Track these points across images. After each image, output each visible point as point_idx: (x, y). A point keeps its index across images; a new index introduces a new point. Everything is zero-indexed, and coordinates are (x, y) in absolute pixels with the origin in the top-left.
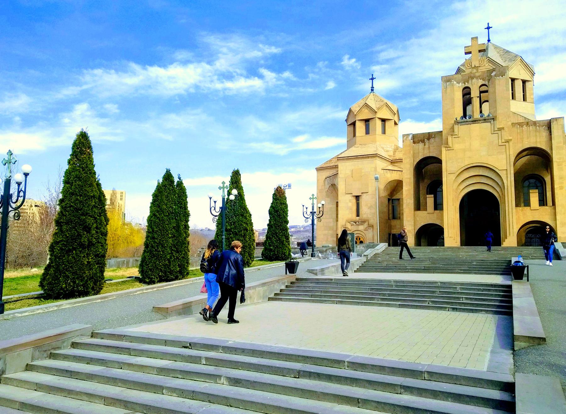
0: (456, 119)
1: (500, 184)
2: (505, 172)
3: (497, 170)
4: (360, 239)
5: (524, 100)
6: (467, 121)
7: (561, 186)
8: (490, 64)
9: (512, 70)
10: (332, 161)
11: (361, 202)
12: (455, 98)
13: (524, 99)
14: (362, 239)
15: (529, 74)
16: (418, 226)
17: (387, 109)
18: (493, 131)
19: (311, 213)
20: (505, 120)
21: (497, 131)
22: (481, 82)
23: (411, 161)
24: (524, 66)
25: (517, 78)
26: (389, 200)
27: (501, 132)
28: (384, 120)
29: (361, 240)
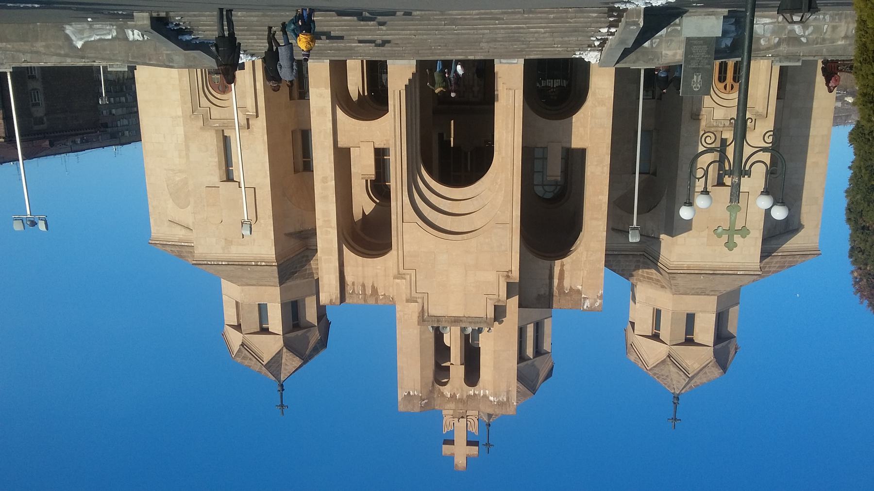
0: (490, 329)
1: (416, 196)
4: (725, 87)
6: (470, 323)
7: (324, 183)
10: (777, 265)
12: (492, 369)
14: (722, 85)
16: (582, 115)
17: (645, 357)
18: (426, 298)
19: (748, 173)
20: (406, 314)
21: (419, 298)
22: (447, 391)
23: (587, 254)
26: (654, 174)
28: (656, 337)
29: (724, 84)
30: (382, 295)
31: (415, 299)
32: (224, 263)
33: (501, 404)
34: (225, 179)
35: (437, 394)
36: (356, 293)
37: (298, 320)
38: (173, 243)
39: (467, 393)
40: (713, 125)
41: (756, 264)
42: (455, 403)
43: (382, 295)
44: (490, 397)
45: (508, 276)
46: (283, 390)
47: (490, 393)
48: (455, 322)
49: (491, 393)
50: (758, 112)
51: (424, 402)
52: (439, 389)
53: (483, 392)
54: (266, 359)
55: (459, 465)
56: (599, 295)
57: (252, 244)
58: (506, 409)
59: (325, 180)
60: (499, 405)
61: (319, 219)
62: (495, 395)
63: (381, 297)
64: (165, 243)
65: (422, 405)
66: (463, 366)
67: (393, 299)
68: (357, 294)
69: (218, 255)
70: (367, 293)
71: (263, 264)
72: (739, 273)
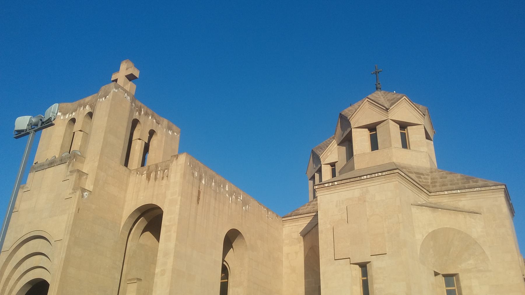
32: (365, 177)
34: (368, 265)
36: (162, 171)
38: (471, 190)
39: (76, 113)
44: (60, 115)
47: (60, 117)
48: (52, 163)
57: (338, 202)
59: (163, 272)
64: (483, 189)
67: (137, 173)
68: (162, 170)
69: (373, 184)
70: (154, 173)
71: (326, 185)
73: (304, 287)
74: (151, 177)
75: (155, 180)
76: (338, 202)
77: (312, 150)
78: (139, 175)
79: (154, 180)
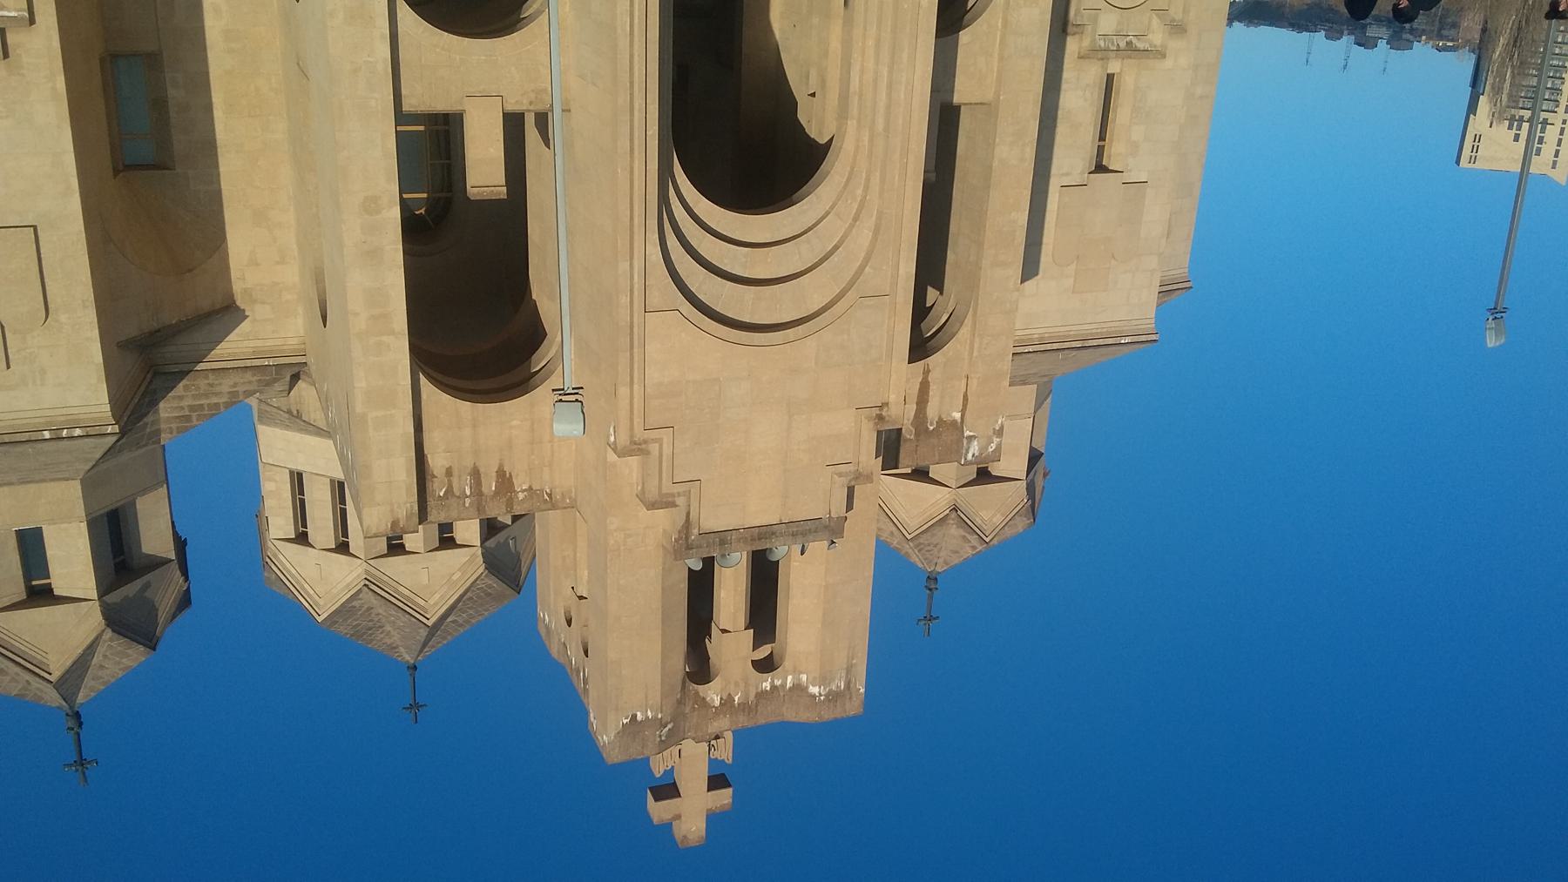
1: (672, 241)
2: (655, 300)
3: (687, 308)
5: (300, 475)
8: (422, 602)
9: (349, 579)
11: (1093, 141)
12: (820, 626)
13: (298, 480)
15: (288, 565)
17: (902, 515)
21: (679, 494)
22: (713, 693)
24: (304, 589)
25: (329, 553)
27: (660, 488)
30: (523, 491)
31: (670, 499)
33: (834, 697)
35: (691, 703)
37: (122, 553)
39: (757, 688)
40: (1100, 46)
41: (1149, 321)
42: (731, 715)
43: (523, 491)
44: (811, 687)
45: (880, 418)
46: (80, 725)
49: (815, 678)
50: (1174, 20)
51: (667, 729)
52: (697, 693)
53: (793, 678)
54: (57, 668)
55: (690, 837)
56: (997, 428)
57: (38, 382)
58: (844, 704)
59: (371, 206)
60: (830, 701)
61: (356, 314)
62: (823, 680)
63: (521, 496)
65: (663, 738)
66: (752, 630)
67: (550, 495)
68: (459, 497)
70: (485, 489)
71: (78, 432)
72: (1123, 342)
73: (222, 169)
74: (494, 479)
75: (478, 471)
76: (38, 382)
77: (519, 593)
78: (542, 490)
79: (482, 470)
